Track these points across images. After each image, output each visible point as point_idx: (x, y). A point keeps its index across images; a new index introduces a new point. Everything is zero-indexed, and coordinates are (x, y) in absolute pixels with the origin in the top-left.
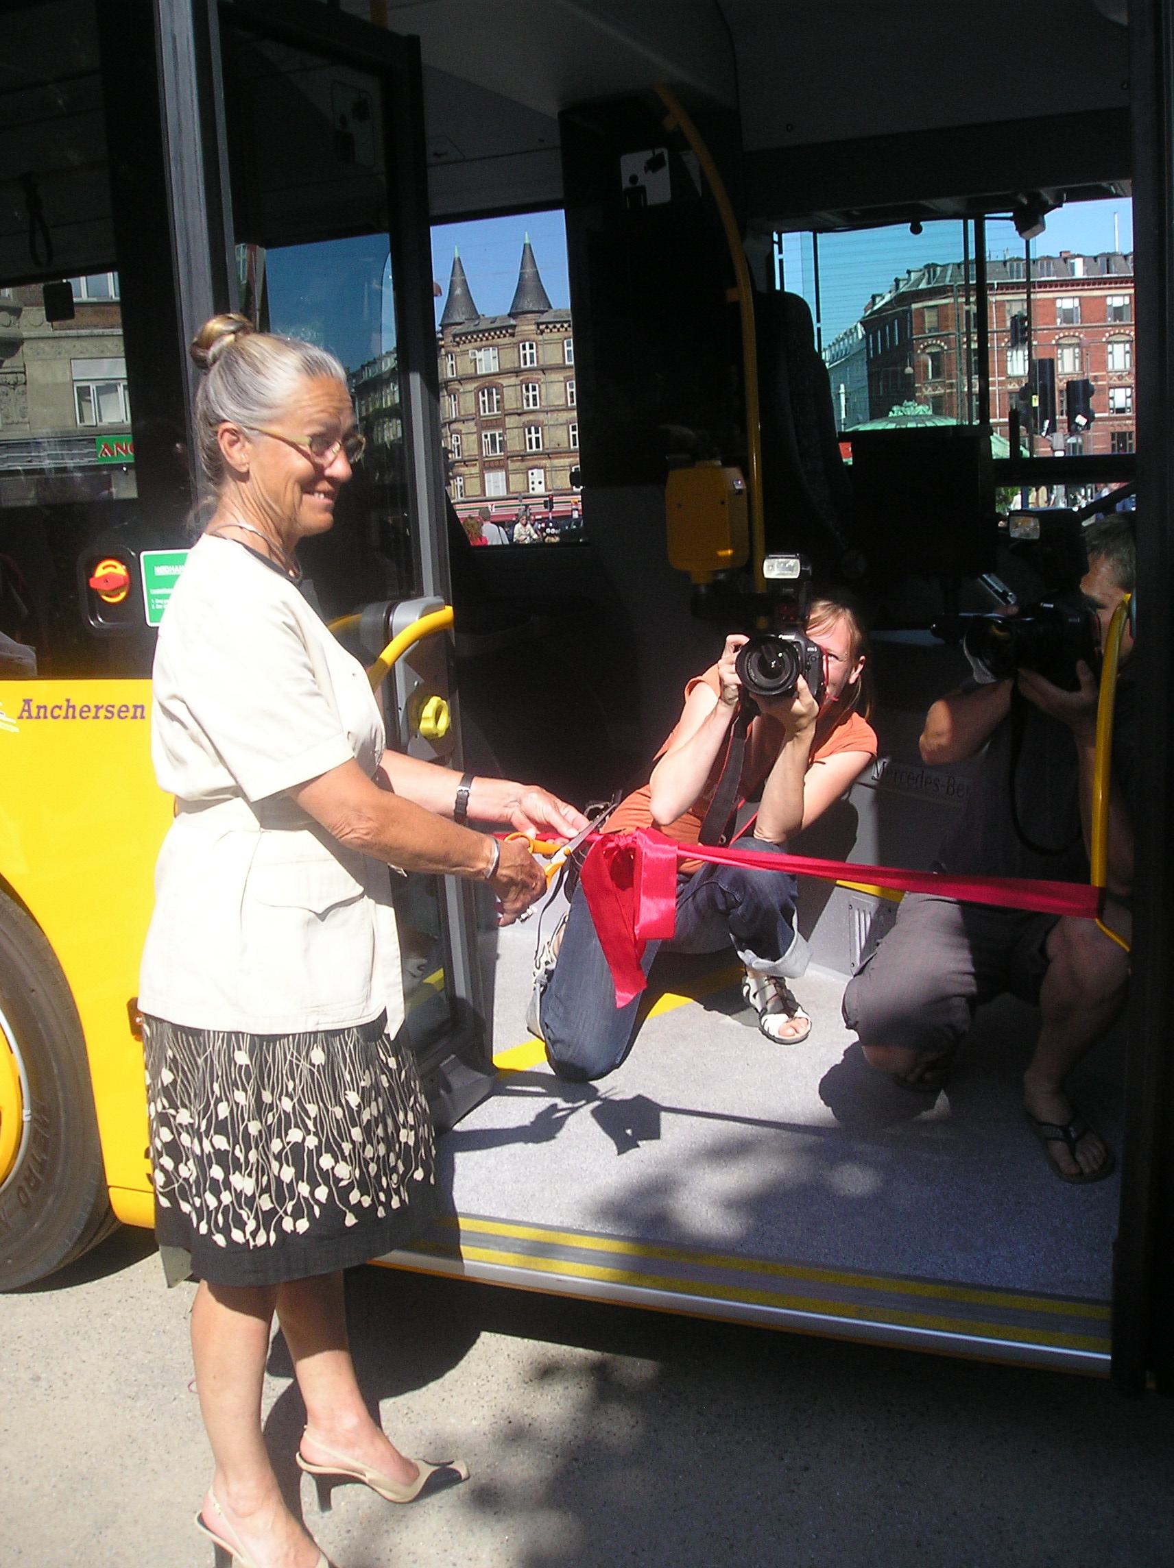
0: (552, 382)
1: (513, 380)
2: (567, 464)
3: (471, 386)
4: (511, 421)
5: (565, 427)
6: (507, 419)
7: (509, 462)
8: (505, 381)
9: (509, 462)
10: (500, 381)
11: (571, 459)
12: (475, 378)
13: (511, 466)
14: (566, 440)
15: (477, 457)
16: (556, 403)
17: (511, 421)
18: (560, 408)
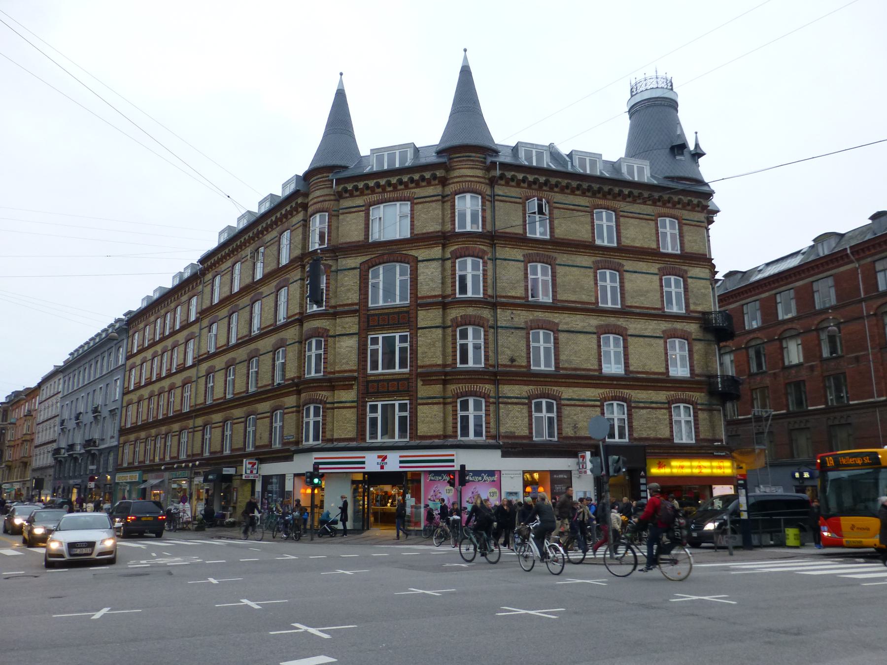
0: (505, 260)
1: (437, 252)
2: (525, 394)
3: (354, 262)
4: (426, 317)
5: (523, 333)
6: (421, 314)
7: (420, 383)
8: (421, 254)
9: (420, 383)
10: (413, 253)
11: (531, 387)
12: (364, 246)
13: (423, 391)
14: (524, 354)
15: (356, 374)
16: (513, 294)
17: (426, 317)
18: (518, 301)
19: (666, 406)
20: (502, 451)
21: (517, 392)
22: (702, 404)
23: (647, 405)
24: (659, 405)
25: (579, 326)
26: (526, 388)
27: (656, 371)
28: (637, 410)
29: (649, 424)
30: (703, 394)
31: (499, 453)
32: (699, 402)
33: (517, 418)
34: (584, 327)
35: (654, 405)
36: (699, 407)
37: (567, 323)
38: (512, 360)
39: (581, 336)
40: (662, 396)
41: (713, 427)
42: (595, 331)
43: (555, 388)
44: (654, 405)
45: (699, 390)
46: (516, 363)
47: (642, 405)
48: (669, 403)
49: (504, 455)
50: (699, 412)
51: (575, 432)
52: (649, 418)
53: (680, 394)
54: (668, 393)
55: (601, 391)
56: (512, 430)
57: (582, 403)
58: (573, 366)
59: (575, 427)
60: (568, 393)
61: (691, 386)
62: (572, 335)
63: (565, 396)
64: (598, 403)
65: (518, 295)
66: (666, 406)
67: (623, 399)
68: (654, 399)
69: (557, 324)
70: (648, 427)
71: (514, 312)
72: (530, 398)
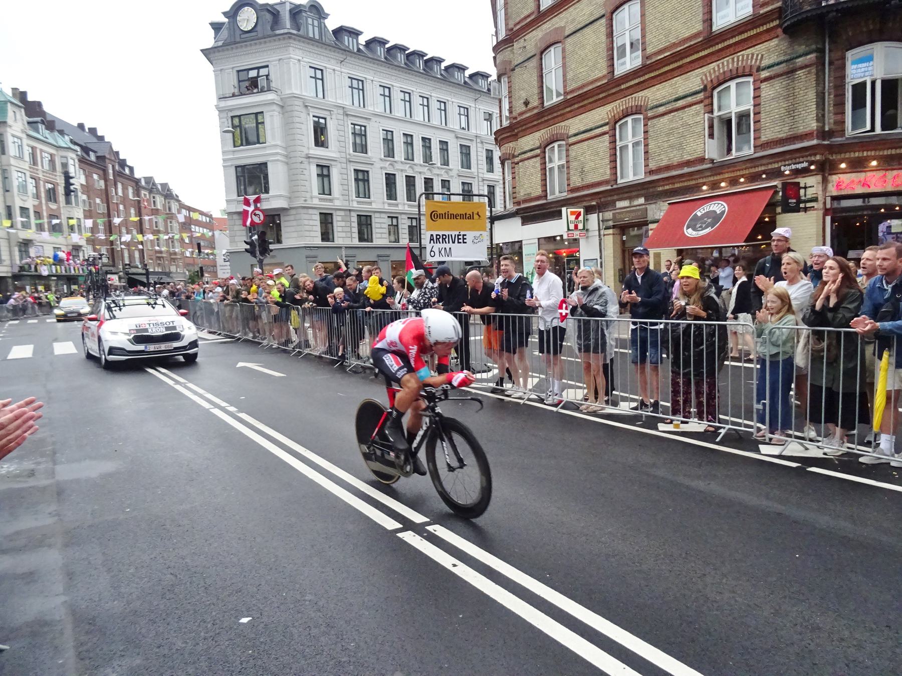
2: (537, 144)
14: (536, 91)
16: (526, 13)
19: (701, 96)
20: (522, 218)
21: (532, 143)
22: (769, 67)
23: (669, 107)
24: (689, 100)
25: (585, 17)
26: (537, 135)
27: (687, 35)
28: (655, 121)
29: (673, 140)
30: (774, 42)
31: (517, 221)
32: (765, 63)
33: (532, 175)
34: (591, 14)
35: (680, 103)
36: (764, 74)
37: (574, 20)
38: (526, 103)
39: (587, 30)
40: (693, 81)
41: (792, 111)
42: (603, 12)
43: (563, 124)
44: (680, 103)
45: (768, 35)
46: (530, 106)
47: (662, 110)
48: (705, 89)
49: (526, 221)
50: (763, 86)
51: (582, 179)
52: (672, 129)
53: (727, 64)
54: (705, 69)
55: (609, 107)
56: (529, 191)
57: (588, 135)
58: (580, 84)
59: (582, 172)
60: (575, 124)
61: (745, 36)
62: (578, 34)
63: (572, 132)
64: (606, 128)
65: (530, 11)
66: (701, 96)
67: (637, 110)
68: (681, 93)
69: (562, 29)
70: (670, 146)
71: (526, 37)
72: (544, 147)
